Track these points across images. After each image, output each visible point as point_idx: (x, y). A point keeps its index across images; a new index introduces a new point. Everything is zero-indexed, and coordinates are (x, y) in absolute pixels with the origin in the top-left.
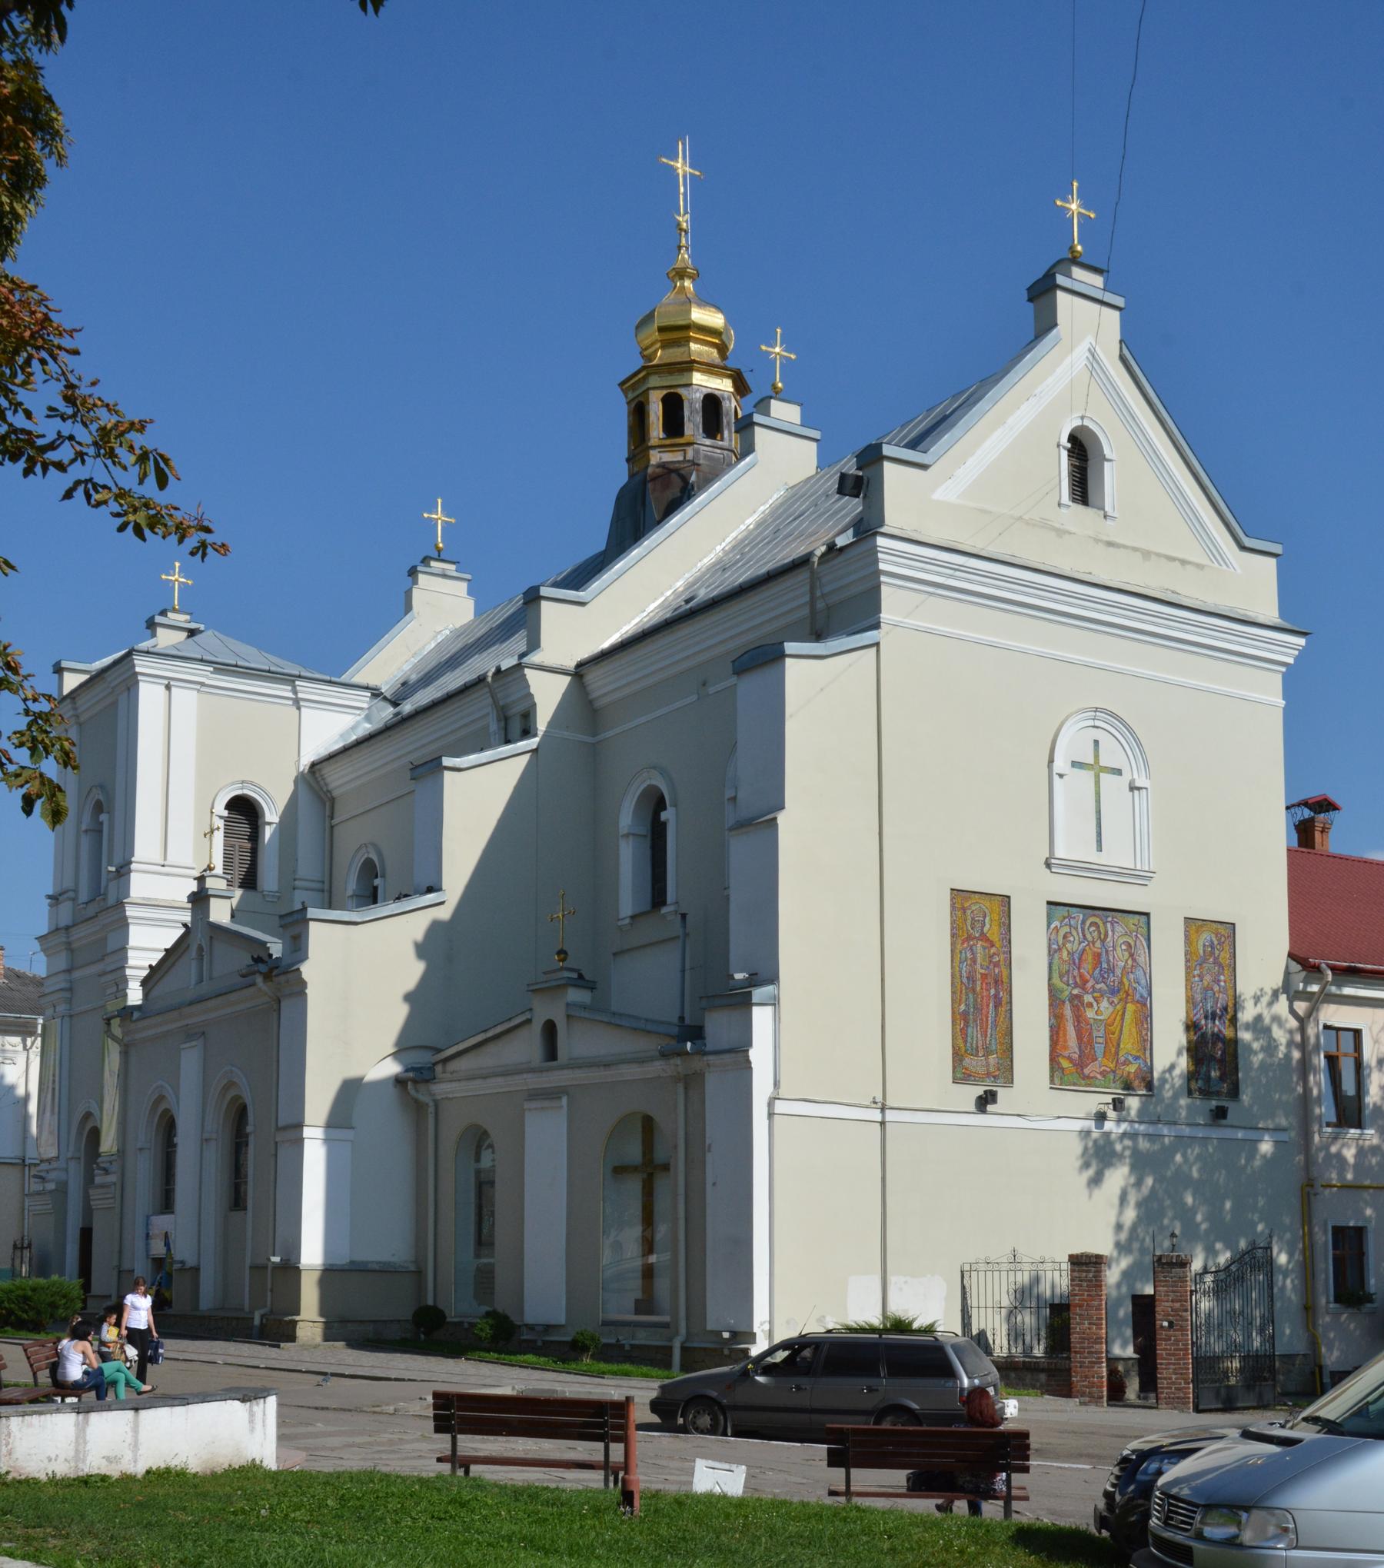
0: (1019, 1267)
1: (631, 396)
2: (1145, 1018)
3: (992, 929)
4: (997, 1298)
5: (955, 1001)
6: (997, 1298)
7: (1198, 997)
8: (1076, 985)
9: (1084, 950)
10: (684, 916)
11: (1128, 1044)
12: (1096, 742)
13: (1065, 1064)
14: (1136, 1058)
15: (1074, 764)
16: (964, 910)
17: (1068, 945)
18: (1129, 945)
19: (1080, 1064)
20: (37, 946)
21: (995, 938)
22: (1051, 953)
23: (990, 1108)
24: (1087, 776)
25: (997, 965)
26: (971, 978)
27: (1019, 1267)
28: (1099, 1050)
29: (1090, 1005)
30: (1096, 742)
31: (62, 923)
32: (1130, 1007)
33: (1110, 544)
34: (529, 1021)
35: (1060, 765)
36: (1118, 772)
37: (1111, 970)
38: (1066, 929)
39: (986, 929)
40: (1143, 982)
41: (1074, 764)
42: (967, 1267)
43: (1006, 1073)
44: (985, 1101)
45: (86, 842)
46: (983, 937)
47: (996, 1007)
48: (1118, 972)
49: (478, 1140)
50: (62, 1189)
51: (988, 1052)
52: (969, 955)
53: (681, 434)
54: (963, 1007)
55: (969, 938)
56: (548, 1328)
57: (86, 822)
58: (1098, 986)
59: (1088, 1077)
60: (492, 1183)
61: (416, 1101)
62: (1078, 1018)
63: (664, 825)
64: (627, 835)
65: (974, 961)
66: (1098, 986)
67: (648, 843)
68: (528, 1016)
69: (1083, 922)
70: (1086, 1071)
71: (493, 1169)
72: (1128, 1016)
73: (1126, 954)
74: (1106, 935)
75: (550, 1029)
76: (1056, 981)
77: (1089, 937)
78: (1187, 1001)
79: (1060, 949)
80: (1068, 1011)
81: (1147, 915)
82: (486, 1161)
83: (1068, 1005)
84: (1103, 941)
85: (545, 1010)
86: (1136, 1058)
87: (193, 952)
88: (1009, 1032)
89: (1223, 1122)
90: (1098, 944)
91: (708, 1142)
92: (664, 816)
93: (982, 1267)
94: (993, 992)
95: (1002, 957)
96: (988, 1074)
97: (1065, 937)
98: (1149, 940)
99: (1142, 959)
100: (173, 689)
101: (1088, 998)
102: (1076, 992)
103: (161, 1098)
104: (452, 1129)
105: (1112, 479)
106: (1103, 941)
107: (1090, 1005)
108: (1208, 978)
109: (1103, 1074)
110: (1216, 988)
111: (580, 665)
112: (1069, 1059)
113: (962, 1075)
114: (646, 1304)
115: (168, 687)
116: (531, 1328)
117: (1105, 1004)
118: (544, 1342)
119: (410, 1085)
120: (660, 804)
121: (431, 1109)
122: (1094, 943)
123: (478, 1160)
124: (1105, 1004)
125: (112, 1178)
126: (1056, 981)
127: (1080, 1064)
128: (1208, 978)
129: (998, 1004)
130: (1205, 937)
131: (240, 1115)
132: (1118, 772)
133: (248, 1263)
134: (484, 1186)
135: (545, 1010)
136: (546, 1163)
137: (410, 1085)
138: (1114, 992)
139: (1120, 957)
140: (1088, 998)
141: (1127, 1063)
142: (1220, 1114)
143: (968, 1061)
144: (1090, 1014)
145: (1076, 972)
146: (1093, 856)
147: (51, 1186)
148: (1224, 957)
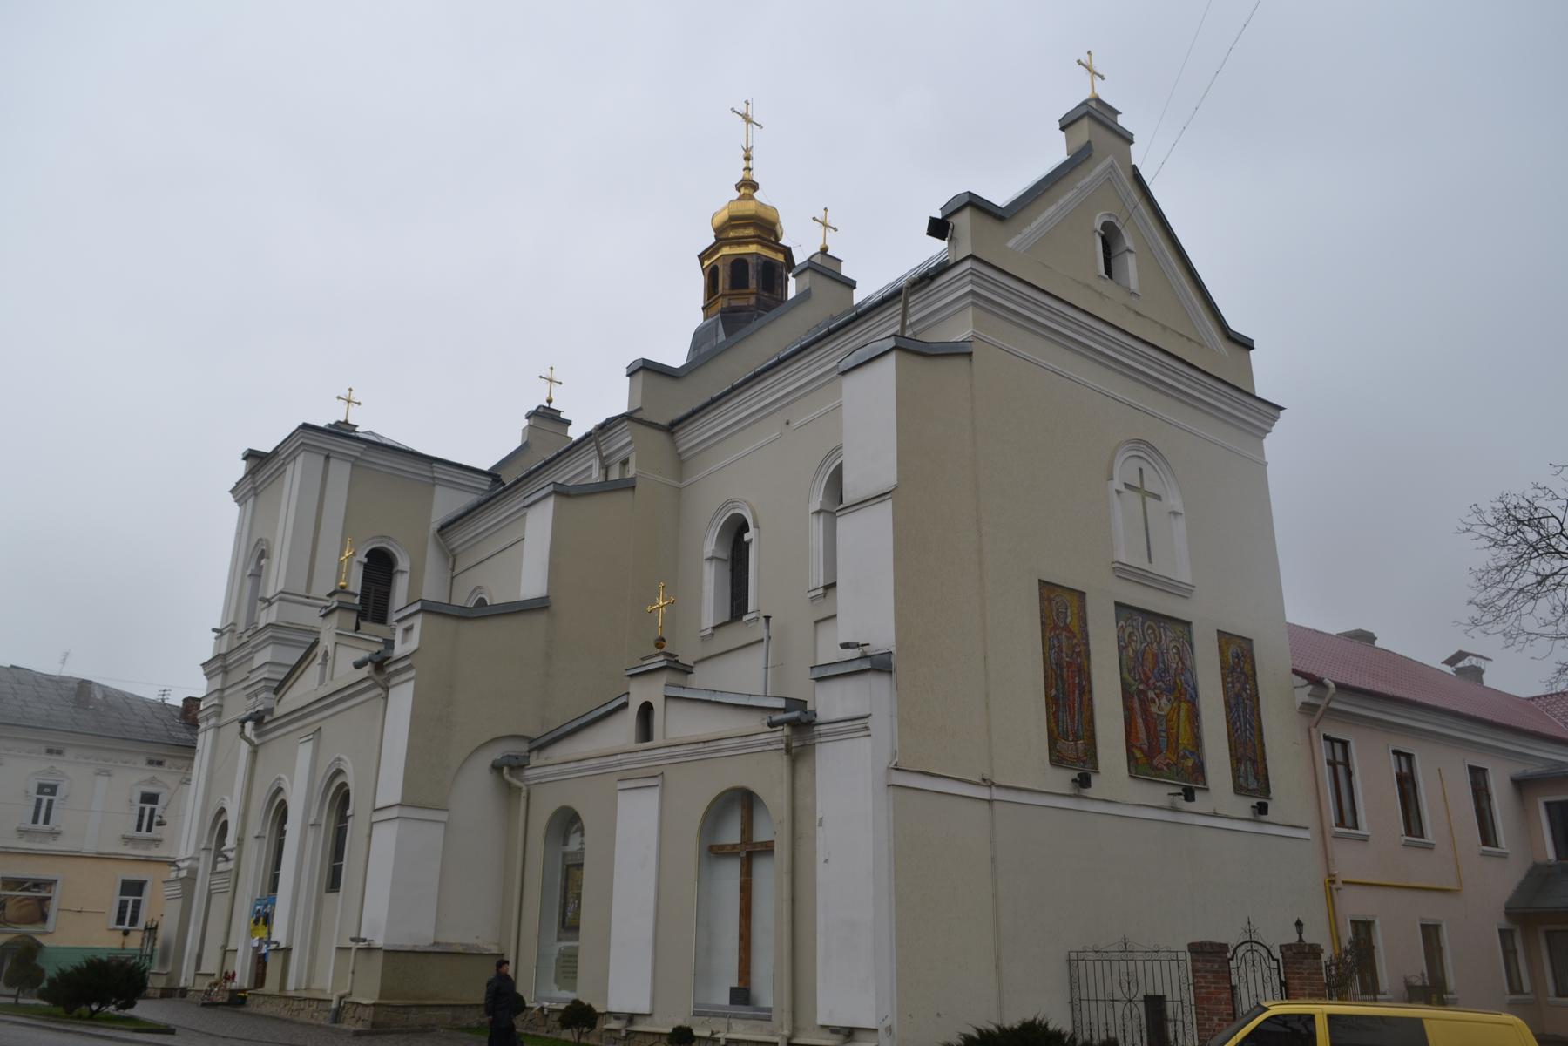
0: (1131, 956)
1: (706, 263)
2: (1194, 717)
4: (1108, 990)
5: (1047, 687)
6: (1108, 990)
7: (1233, 701)
10: (768, 618)
11: (1184, 739)
13: (1138, 754)
16: (1050, 600)
19: (1150, 754)
20: (201, 670)
21: (1075, 629)
22: (1121, 649)
23: (1087, 792)
24: (1134, 498)
25: (1079, 654)
26: (1059, 664)
27: (1131, 956)
28: (1163, 742)
31: (223, 651)
32: (1184, 705)
33: (1138, 314)
34: (625, 705)
35: (1117, 484)
36: (1158, 497)
37: (1167, 670)
42: (1073, 956)
44: (1083, 781)
45: (248, 583)
46: (1067, 628)
47: (1081, 695)
48: (1172, 672)
49: (567, 821)
50: (193, 873)
51: (1076, 739)
53: (747, 287)
55: (1055, 627)
56: (631, 1018)
57: (252, 567)
59: (1156, 768)
60: (580, 866)
61: (509, 785)
62: (1146, 711)
63: (747, 544)
64: (711, 559)
67: (728, 567)
68: (623, 700)
70: (1155, 762)
71: (581, 852)
72: (1182, 713)
75: (646, 710)
76: (1126, 675)
80: (1137, 705)
81: (1188, 624)
82: (574, 844)
83: (1136, 700)
84: (1159, 643)
85: (639, 693)
86: (1192, 753)
87: (319, 660)
88: (1091, 721)
89: (1264, 818)
91: (819, 816)
92: (747, 537)
93: (1091, 956)
96: (1078, 759)
98: (1191, 645)
99: (1188, 663)
100: (332, 461)
101: (1151, 694)
103: (280, 790)
104: (544, 808)
105: (1131, 267)
108: (1238, 686)
109: (1168, 765)
111: (674, 424)
112: (1141, 749)
113: (1057, 759)
114: (742, 995)
115: (327, 458)
116: (617, 1016)
118: (629, 1033)
119: (506, 770)
120: (744, 527)
121: (524, 794)
123: (565, 843)
124: (1164, 701)
125: (231, 865)
126: (1126, 675)
127: (1150, 754)
128: (1238, 686)
129: (1082, 693)
130: (1232, 649)
131: (342, 799)
132: (1158, 497)
133: (335, 945)
134: (572, 869)
135: (639, 693)
136: (638, 843)
137: (506, 770)
139: (1172, 659)
141: (1185, 757)
142: (1262, 809)
143: (1061, 744)
144: (1154, 709)
146: (1146, 567)
147: (183, 874)
148: (1247, 667)
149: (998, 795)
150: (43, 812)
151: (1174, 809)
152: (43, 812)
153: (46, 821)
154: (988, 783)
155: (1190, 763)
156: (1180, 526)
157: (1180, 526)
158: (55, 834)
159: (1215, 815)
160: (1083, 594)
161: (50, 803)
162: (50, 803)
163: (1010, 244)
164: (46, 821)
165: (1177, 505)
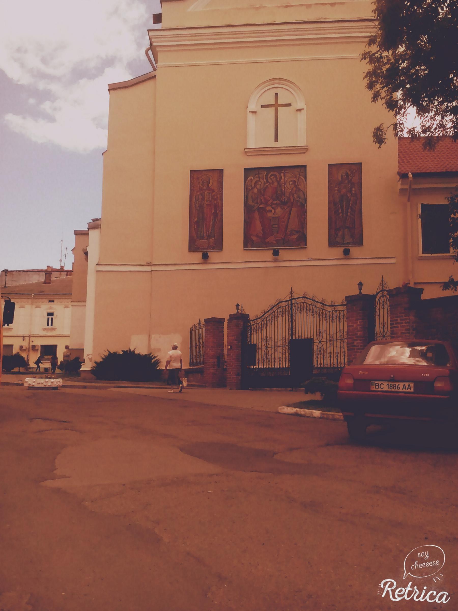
3: (213, 184)
8: (262, 203)
9: (267, 187)
12: (276, 94)
13: (254, 238)
14: (297, 232)
15: (263, 106)
17: (258, 187)
18: (294, 182)
29: (270, 211)
30: (276, 94)
32: (294, 209)
36: (290, 105)
38: (258, 179)
39: (210, 185)
40: (302, 197)
41: (263, 106)
43: (218, 246)
46: (208, 188)
48: (287, 194)
51: (209, 237)
52: (200, 197)
54: (196, 220)
58: (275, 202)
65: (203, 199)
66: (275, 202)
69: (267, 175)
70: (267, 240)
73: (293, 186)
74: (281, 178)
77: (270, 181)
78: (329, 203)
79: (253, 188)
80: (257, 215)
81: (305, 166)
84: (279, 182)
86: (297, 232)
90: (276, 183)
94: (213, 211)
95: (219, 196)
97: (256, 183)
102: (261, 206)
106: (279, 182)
107: (270, 211)
110: (349, 195)
117: (279, 210)
122: (273, 183)
124: (279, 210)
126: (250, 202)
132: (290, 105)
138: (284, 203)
140: (268, 208)
145: (262, 198)
146: (274, 145)
149: (154, 268)
150: (50, 322)
151: (276, 261)
152: (50, 322)
153: (52, 325)
154: (149, 264)
155: (295, 237)
156: (302, 117)
157: (302, 117)
158: (54, 329)
159: (310, 260)
160: (221, 171)
161: (52, 319)
162: (52, 319)
163: (189, 10)
164: (52, 325)
165: (301, 104)
